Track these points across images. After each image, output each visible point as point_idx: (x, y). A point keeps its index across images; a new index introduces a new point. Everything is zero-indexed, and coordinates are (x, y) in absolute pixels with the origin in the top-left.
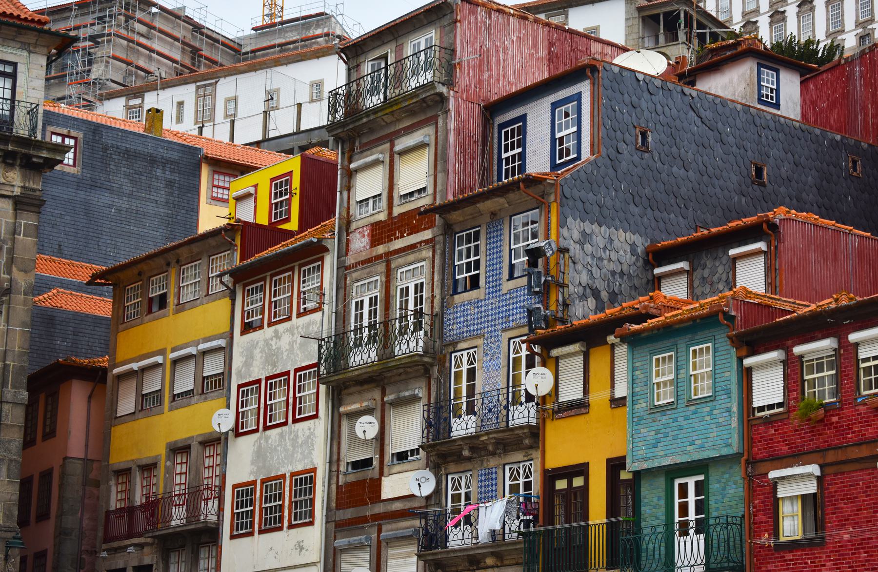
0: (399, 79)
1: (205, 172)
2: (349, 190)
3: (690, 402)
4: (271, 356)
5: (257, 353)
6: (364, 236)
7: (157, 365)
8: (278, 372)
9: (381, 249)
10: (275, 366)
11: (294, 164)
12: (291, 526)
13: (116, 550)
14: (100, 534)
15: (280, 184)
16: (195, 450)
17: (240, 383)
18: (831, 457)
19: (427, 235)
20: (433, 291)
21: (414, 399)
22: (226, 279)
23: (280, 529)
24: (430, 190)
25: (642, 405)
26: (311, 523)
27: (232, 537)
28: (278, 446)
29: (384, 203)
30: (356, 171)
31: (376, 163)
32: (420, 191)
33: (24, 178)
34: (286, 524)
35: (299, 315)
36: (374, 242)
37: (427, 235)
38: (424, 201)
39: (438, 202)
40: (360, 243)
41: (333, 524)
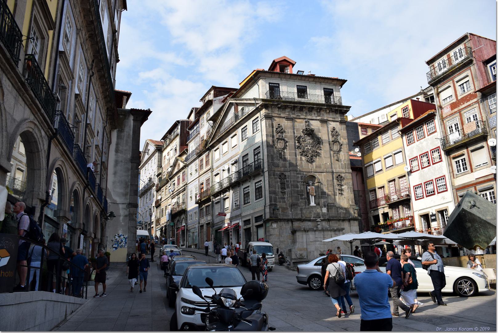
0: (450, 63)
1: (359, 128)
2: (439, 97)
7: (380, 161)
9: (456, 110)
11: (409, 103)
12: (438, 193)
13: (375, 210)
14: (368, 207)
15: (405, 110)
16: (397, 180)
19: (475, 100)
21: (482, 147)
22: (400, 133)
23: (434, 194)
26: (447, 191)
27: (416, 200)
29: (454, 97)
30: (440, 92)
31: (449, 87)
33: (341, 116)
34: (436, 192)
35: (428, 135)
36: (452, 109)
37: (475, 100)
39: (477, 89)
40: (447, 111)
41: (455, 190)
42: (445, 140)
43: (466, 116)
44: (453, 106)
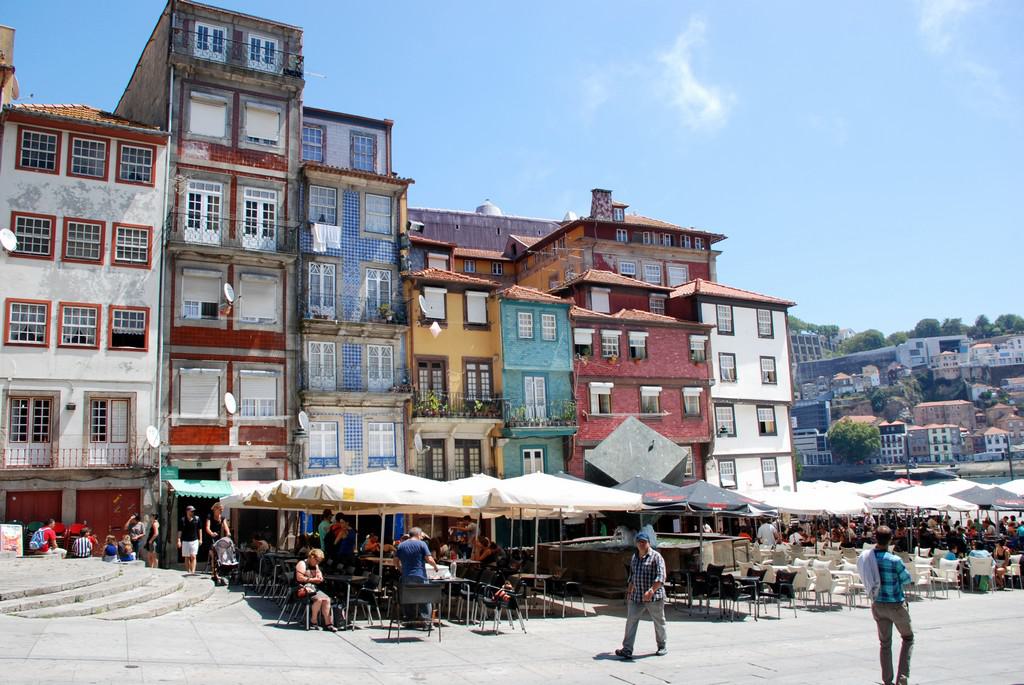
3: (543, 341)
4: (68, 202)
5: (46, 192)
6: (201, 149)
8: (84, 217)
9: (224, 166)
10: (79, 210)
17: (16, 209)
18: (618, 381)
19: (280, 174)
20: (286, 213)
24: (282, 145)
25: (512, 336)
28: (88, 279)
32: (266, 141)
34: (103, 344)
38: (279, 150)
42: (173, 218)
43: (245, 196)
44: (216, 150)
